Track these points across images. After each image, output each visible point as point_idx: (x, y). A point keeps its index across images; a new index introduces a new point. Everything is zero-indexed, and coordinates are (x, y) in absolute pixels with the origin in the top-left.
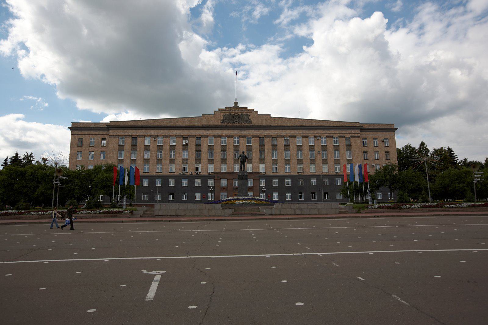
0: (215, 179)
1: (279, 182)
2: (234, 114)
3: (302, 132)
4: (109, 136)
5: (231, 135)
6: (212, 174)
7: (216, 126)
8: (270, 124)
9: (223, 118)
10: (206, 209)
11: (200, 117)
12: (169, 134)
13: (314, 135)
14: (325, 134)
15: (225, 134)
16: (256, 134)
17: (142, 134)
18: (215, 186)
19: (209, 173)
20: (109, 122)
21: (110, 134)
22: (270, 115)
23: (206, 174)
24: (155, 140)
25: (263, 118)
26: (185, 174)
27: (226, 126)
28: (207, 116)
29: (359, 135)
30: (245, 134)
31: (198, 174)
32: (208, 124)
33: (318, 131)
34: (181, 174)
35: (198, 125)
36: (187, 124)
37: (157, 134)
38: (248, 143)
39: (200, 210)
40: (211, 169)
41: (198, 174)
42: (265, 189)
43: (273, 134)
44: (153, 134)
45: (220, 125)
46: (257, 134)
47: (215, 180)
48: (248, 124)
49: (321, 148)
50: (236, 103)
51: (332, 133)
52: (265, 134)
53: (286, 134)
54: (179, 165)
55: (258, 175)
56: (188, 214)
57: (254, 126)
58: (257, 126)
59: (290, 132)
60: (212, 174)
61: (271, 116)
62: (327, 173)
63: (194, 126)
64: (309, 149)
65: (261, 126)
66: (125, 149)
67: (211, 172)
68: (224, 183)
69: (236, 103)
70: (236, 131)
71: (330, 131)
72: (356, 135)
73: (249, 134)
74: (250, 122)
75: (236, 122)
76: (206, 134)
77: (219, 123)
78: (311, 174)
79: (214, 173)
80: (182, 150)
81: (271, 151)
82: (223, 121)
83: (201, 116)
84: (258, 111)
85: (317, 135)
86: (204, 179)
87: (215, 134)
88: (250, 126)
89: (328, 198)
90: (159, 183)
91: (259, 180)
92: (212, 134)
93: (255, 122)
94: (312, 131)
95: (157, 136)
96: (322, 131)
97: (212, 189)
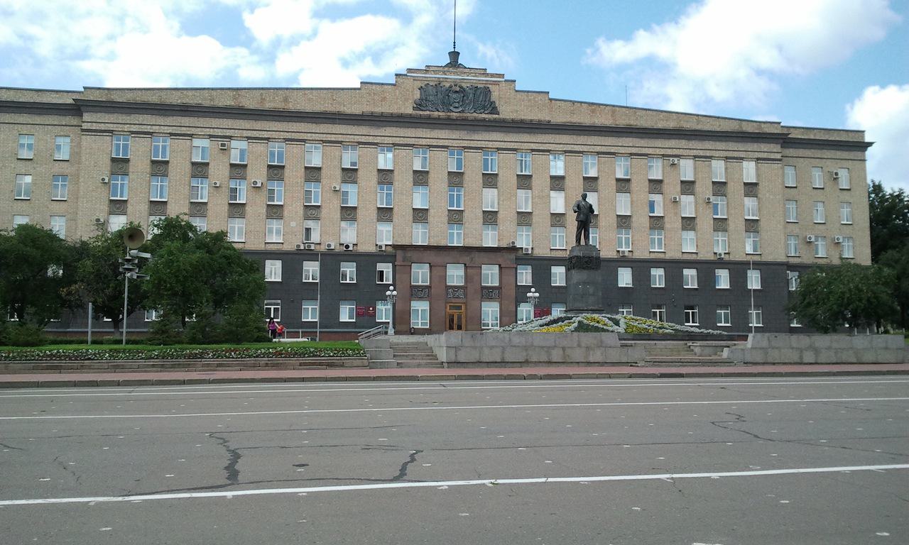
0: (396, 263)
1: (635, 278)
2: (451, 87)
4: (83, 130)
5: (441, 143)
6: (390, 249)
7: (401, 116)
8: (547, 119)
10: (579, 346)
11: (355, 89)
12: (266, 135)
14: (692, 151)
15: (424, 142)
17: (184, 130)
19: (381, 247)
20: (83, 90)
21: (85, 126)
23: (372, 249)
24: (224, 150)
25: (530, 100)
26: (313, 248)
27: (429, 117)
28: (374, 87)
29: (778, 156)
30: (479, 144)
31: (351, 248)
32: (378, 109)
34: (302, 248)
36: (318, 108)
37: (228, 133)
38: (486, 168)
39: (564, 349)
40: (386, 235)
41: (351, 248)
42: (537, 295)
44: (219, 132)
45: (410, 116)
46: (513, 144)
47: (397, 267)
49: (678, 188)
50: (454, 55)
54: (293, 224)
55: (513, 256)
56: (534, 359)
57: (504, 121)
58: (513, 121)
60: (390, 249)
61: (551, 96)
62: (694, 256)
63: (339, 114)
64: (647, 189)
65: (522, 121)
66: (131, 170)
67: (386, 245)
68: (421, 274)
69: (454, 55)
70: (456, 134)
71: (704, 142)
72: (772, 156)
73: (491, 143)
74: (494, 110)
75: (454, 110)
76: (371, 139)
77: (408, 109)
78: (653, 256)
79: (395, 247)
80: (303, 180)
82: (419, 105)
85: (669, 152)
86: (366, 262)
87: (397, 141)
88: (495, 121)
91: (516, 268)
93: (506, 112)
94: (659, 143)
95: (230, 137)
96: (683, 143)
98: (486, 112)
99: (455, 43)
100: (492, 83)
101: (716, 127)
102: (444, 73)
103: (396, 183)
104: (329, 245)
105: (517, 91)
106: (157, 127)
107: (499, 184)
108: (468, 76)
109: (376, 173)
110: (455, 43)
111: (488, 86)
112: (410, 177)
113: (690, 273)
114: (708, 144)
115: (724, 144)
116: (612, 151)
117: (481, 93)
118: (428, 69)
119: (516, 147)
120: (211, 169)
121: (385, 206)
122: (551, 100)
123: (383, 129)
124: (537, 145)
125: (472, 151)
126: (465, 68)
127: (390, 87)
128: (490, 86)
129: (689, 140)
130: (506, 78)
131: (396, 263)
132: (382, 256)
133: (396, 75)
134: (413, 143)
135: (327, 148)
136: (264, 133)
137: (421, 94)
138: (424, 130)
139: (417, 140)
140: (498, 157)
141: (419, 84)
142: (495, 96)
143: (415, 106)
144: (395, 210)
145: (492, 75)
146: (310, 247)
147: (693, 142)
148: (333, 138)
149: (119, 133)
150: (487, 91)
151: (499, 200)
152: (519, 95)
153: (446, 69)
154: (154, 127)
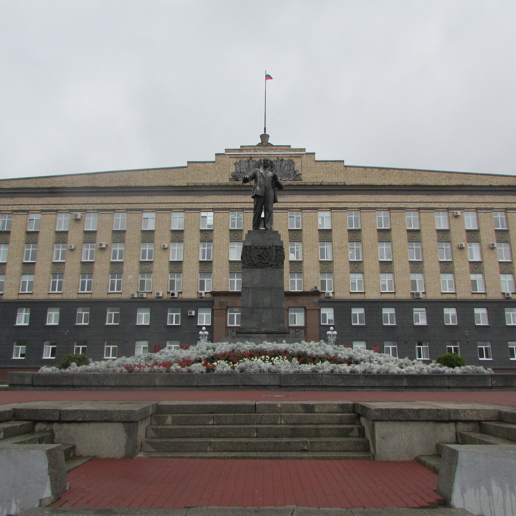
0: (214, 308)
3: (418, 200)
6: (209, 296)
9: (234, 169)
12: (112, 207)
13: (447, 206)
14: (474, 204)
15: (238, 206)
16: (312, 204)
18: (215, 324)
22: (343, 161)
25: (327, 168)
28: (198, 165)
31: (176, 296)
32: (200, 181)
33: (456, 198)
34: (136, 296)
35: (178, 185)
41: (176, 296)
42: (335, 332)
43: (352, 204)
45: (227, 186)
46: (314, 204)
47: (215, 311)
49: (464, 236)
50: (264, 137)
51: (490, 201)
52: (331, 204)
53: (381, 204)
55: (316, 299)
57: (305, 185)
59: (390, 201)
60: (209, 296)
64: (436, 238)
66: (11, 240)
67: (206, 293)
69: (264, 137)
71: (484, 196)
73: (295, 204)
74: (297, 176)
76: (194, 206)
77: (226, 180)
78: (445, 297)
80: (140, 241)
81: (345, 241)
83: (186, 165)
84: (314, 154)
85: (453, 206)
87: (216, 206)
89: (487, 357)
90: (53, 318)
91: (319, 311)
92: (210, 206)
93: (308, 178)
96: (465, 198)
97: (207, 333)
98: (290, 179)
99: (265, 128)
100: (295, 156)
101: (495, 182)
102: (255, 151)
103: (215, 241)
104: (158, 294)
105: (316, 161)
106: (32, 206)
107: (304, 237)
108: (275, 152)
109: (198, 233)
110: (265, 128)
112: (227, 234)
113: (450, 312)
114: (489, 198)
115: (502, 197)
116: (402, 206)
117: (286, 164)
118: (243, 148)
119: (317, 206)
120: (70, 236)
121: (206, 260)
123: (205, 198)
124: (335, 204)
125: (279, 211)
126: (273, 146)
127: (211, 164)
128: (294, 159)
129: (470, 195)
130: (307, 151)
131: (214, 308)
132: (200, 303)
133: (216, 154)
134: (230, 207)
135: (159, 215)
136: (110, 205)
137: (236, 168)
138: (239, 196)
141: (235, 160)
142: (297, 166)
143: (231, 177)
144: (214, 263)
145: (295, 150)
146: (143, 295)
147: (474, 197)
148: (164, 206)
149: (5, 212)
150: (291, 163)
151: (303, 251)
152: (318, 164)
153: (257, 147)
154: (30, 206)
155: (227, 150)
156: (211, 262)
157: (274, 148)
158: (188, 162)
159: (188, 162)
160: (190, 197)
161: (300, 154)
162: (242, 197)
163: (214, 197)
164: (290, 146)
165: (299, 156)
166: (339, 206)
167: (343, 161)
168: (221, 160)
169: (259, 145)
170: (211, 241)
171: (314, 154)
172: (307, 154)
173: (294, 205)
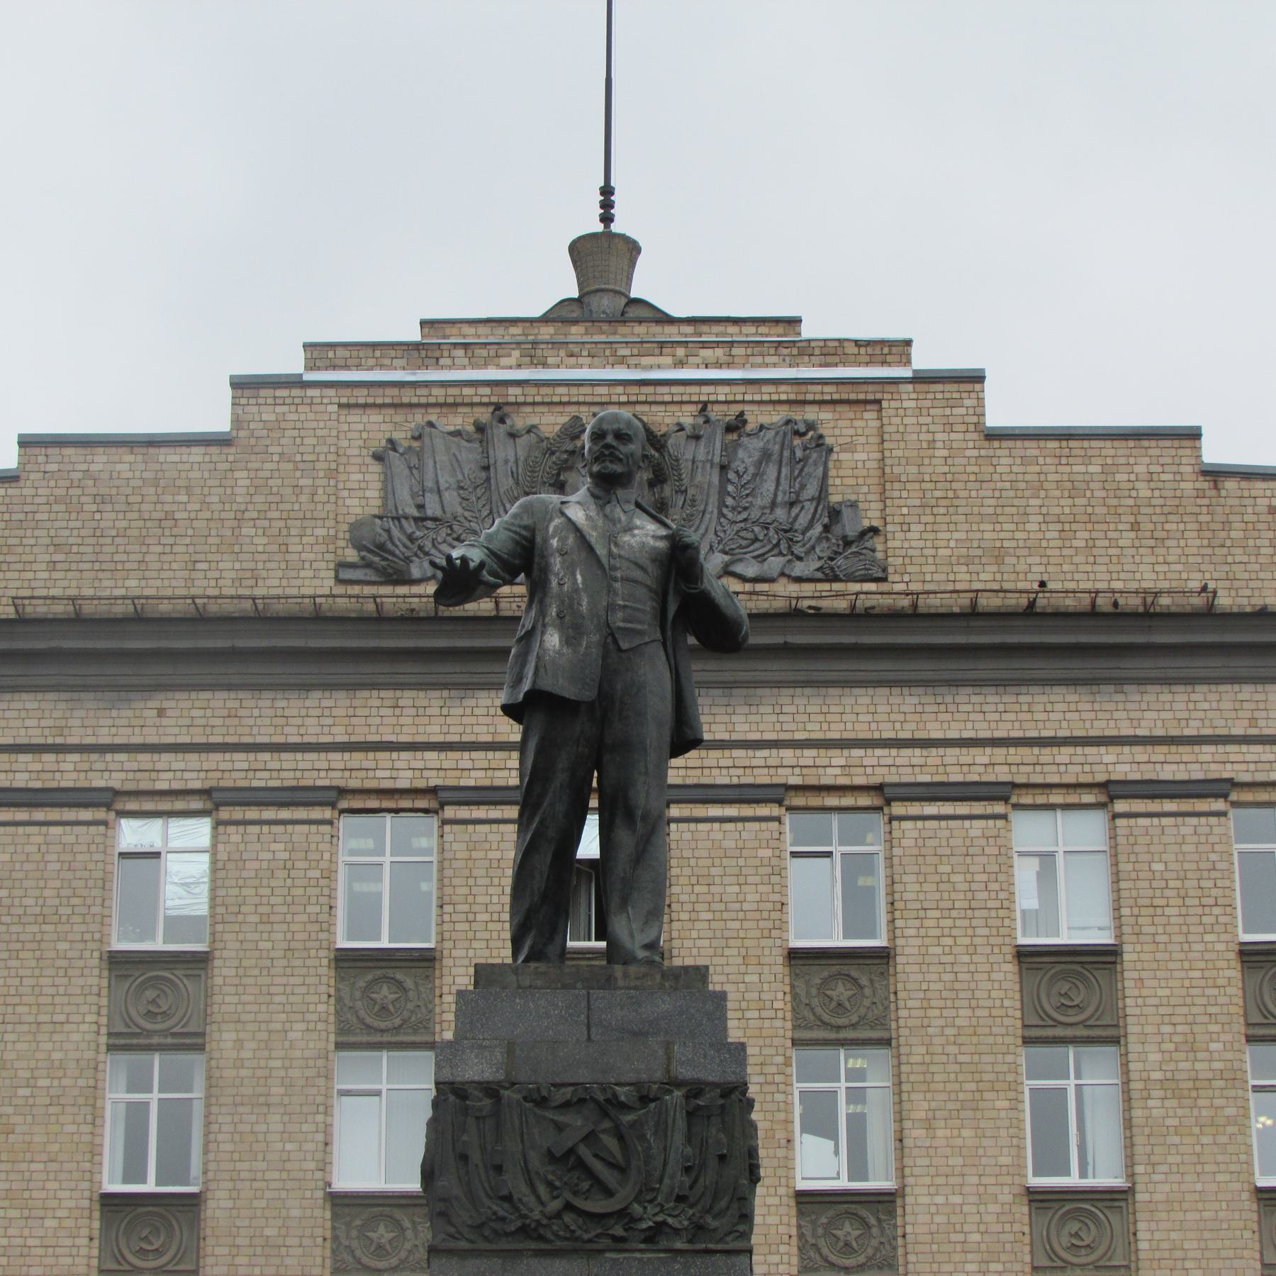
9: (374, 494)
15: (403, 771)
16: (966, 755)
25: (1074, 489)
28: (99, 461)
45: (318, 619)
46: (982, 756)
48: (808, 595)
50: (603, 255)
52: (1108, 755)
57: (913, 616)
61: (1214, 452)
69: (603, 255)
73: (838, 758)
76: (69, 772)
77: (307, 574)
81: (1224, 1041)
84: (977, 378)
87: (236, 770)
88: (857, 617)
93: (930, 561)
98: (799, 569)
99: (607, 191)
100: (830, 392)
102: (533, 354)
103: (223, 1040)
107: (908, 1012)
108: (680, 364)
109: (96, 978)
110: (607, 191)
111: (811, 413)
112: (316, 992)
117: (766, 455)
119: (1002, 774)
121: (150, 1186)
122: (1216, 475)
124: (1140, 753)
126: (665, 319)
127: (197, 454)
130: (923, 360)
133: (239, 384)
134: (337, 779)
138: (407, 698)
139: (356, 759)
140: (890, 842)
141: (378, 428)
142: (852, 472)
143: (351, 555)
144: (216, 1210)
145: (833, 350)
150: (805, 447)
152: (1005, 458)
153: (547, 332)
155: (318, 352)
156: (192, 1203)
157: (671, 333)
158: (26, 442)
159: (26, 442)
160: (29, 701)
161: (876, 377)
162: (433, 701)
163: (221, 701)
164: (794, 322)
165: (864, 398)
166: (1167, 773)
167: (1193, 435)
168: (278, 425)
169: (561, 314)
170: (193, 1042)
171: (977, 378)
172: (923, 379)
173: (834, 766)
